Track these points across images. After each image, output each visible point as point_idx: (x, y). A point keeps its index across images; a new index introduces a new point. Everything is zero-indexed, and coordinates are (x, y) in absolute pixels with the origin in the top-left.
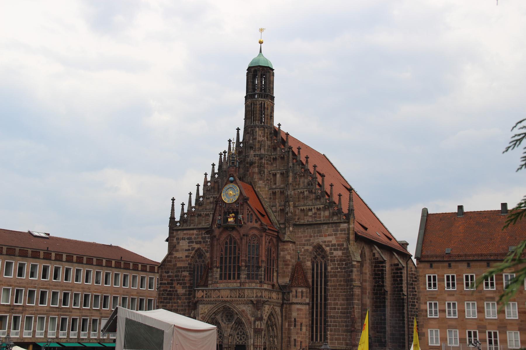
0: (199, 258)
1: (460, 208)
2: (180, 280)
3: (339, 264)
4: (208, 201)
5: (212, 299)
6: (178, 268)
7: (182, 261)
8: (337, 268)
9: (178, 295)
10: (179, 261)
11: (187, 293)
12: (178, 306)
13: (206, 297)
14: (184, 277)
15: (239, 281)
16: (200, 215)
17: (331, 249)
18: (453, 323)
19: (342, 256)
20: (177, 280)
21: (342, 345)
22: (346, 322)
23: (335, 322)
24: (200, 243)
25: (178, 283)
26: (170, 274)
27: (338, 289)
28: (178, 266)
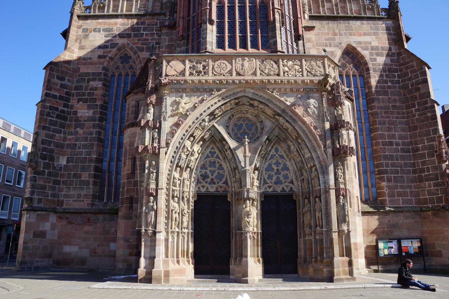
0: (122, 63)
2: (84, 94)
8: (386, 82)
9: (77, 120)
10: (84, 64)
11: (98, 116)
12: (76, 140)
13: (191, 74)
14: (92, 89)
17: (371, 54)
19: (391, 65)
20: (78, 94)
21: (411, 203)
22: (413, 165)
23: (393, 165)
26: (66, 82)
27: (392, 113)
28: (81, 71)
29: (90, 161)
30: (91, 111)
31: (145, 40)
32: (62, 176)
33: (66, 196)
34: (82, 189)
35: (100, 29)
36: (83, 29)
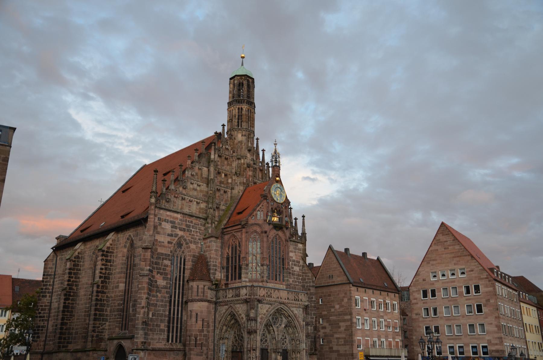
1: (347, 250)
3: (297, 279)
4: (191, 186)
5: (273, 299)
6: (158, 254)
7: (164, 246)
11: (169, 286)
12: (157, 301)
14: (165, 266)
15: (284, 283)
16: (183, 199)
17: (292, 264)
18: (367, 333)
20: (157, 269)
24: (184, 230)
25: (158, 273)
29: (165, 316)
30: (165, 282)
31: (193, 235)
32: (150, 324)
33: (152, 339)
34: (161, 334)
35: (168, 220)
36: (159, 218)
